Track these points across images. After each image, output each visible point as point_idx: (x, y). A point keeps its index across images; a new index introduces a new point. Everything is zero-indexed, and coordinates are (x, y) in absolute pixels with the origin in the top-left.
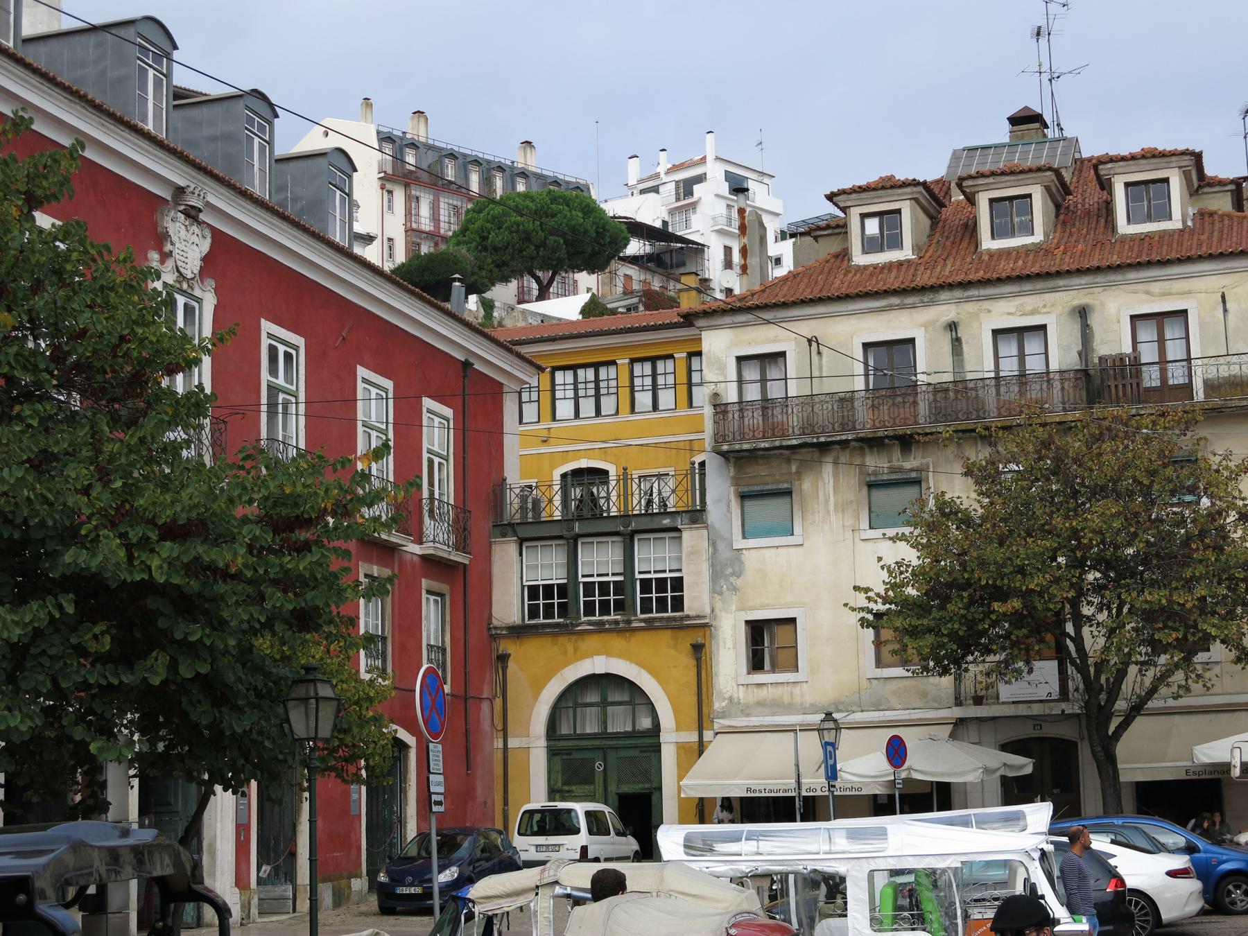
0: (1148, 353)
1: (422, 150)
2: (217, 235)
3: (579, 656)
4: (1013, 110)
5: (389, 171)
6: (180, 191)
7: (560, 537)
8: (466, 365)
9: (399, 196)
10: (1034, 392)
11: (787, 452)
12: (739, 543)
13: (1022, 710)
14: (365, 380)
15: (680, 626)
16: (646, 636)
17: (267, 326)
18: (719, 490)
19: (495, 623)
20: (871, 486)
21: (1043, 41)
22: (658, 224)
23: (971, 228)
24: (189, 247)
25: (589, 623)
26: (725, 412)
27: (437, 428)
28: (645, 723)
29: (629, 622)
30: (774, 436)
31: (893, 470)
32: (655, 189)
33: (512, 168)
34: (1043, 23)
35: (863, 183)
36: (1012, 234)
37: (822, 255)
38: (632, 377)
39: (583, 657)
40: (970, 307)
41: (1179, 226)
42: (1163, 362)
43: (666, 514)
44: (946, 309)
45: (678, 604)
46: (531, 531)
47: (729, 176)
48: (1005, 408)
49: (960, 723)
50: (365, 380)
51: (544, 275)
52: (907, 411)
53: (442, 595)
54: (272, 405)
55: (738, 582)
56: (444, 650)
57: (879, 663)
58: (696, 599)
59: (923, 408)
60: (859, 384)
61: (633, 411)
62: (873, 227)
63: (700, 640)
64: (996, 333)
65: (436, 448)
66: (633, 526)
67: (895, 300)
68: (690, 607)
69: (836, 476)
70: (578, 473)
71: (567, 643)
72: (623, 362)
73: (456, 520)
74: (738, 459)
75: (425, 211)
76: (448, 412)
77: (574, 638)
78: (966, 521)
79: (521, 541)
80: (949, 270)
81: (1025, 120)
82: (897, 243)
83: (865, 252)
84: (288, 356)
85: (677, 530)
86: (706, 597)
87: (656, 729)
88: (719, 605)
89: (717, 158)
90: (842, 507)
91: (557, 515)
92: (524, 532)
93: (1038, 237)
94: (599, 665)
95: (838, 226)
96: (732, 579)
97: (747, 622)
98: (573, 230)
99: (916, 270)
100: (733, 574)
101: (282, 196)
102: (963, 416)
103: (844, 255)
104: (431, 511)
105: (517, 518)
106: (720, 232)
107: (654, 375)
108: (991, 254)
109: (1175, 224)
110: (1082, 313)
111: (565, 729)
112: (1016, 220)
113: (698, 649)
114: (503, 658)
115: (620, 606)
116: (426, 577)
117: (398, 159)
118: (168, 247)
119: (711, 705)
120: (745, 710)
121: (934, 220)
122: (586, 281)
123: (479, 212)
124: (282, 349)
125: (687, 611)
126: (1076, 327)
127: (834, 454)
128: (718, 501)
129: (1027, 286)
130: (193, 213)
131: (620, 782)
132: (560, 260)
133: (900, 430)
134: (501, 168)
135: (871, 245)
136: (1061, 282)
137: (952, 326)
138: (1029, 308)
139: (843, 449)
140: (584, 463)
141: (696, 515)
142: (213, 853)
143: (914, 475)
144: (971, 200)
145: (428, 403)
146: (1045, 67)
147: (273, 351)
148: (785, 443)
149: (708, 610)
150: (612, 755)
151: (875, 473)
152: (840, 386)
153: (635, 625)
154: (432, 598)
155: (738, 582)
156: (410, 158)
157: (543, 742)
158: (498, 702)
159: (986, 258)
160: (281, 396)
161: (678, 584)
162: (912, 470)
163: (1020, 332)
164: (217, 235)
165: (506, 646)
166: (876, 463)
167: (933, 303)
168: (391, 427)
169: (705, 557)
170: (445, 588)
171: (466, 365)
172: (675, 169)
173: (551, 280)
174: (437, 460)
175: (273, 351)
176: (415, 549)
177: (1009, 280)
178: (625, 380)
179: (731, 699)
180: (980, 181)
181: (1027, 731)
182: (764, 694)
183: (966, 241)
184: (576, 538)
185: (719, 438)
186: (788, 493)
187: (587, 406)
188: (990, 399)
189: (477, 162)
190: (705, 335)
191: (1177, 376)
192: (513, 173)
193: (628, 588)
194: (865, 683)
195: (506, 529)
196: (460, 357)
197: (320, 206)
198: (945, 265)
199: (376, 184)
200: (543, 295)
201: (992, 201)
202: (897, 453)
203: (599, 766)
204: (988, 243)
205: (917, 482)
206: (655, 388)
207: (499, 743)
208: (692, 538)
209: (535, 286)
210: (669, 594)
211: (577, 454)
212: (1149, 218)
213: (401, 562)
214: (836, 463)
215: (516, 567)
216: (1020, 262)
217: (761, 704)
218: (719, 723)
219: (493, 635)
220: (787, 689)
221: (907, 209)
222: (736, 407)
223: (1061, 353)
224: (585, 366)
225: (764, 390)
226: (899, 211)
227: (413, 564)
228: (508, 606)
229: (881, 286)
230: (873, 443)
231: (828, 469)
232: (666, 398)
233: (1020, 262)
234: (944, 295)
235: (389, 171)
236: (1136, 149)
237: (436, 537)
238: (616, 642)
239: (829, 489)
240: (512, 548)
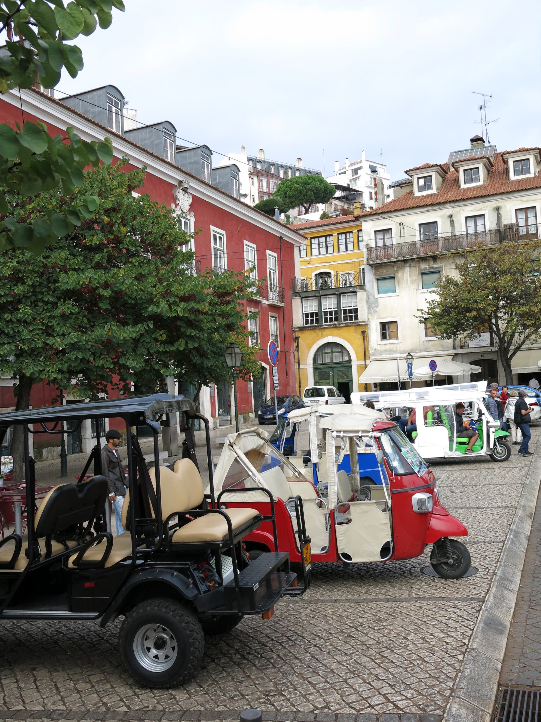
0: (522, 222)
1: (263, 163)
2: (194, 197)
3: (323, 337)
4: (472, 136)
5: (252, 171)
6: (181, 182)
7: (315, 296)
8: (281, 238)
9: (256, 179)
10: (480, 239)
11: (393, 264)
12: (377, 296)
13: (477, 350)
14: (246, 245)
15: (357, 325)
16: (346, 328)
17: (212, 228)
18: (370, 277)
19: (294, 326)
20: (422, 274)
21: (483, 110)
22: (346, 185)
23: (457, 181)
25: (326, 325)
26: (371, 250)
27: (272, 260)
28: (346, 358)
29: (340, 324)
30: (388, 258)
31: (430, 268)
32: (345, 173)
33: (294, 168)
34: (483, 104)
35: (418, 166)
36: (472, 182)
37: (404, 193)
38: (338, 240)
39: (324, 337)
40: (457, 209)
41: (533, 176)
42: (527, 225)
43: (351, 286)
44: (448, 210)
45: (356, 317)
46: (305, 294)
47: (371, 167)
48: (470, 245)
49: (455, 355)
50: (246, 245)
51: (307, 205)
52: (435, 247)
53: (276, 318)
54: (216, 255)
55: (377, 309)
56: (277, 336)
57: (427, 335)
58: (362, 316)
59: (441, 246)
60: (418, 238)
61: (339, 251)
62: (422, 182)
63: (364, 330)
64: (466, 218)
65: (272, 267)
66: (340, 291)
67: (430, 208)
68: (360, 318)
69: (410, 271)
70: (320, 274)
71: (318, 332)
72: (335, 234)
73: (280, 292)
74: (376, 267)
75: (265, 184)
77: (321, 330)
78: (456, 285)
79: (302, 298)
80: (449, 196)
81: (477, 140)
82: (430, 187)
83: (419, 191)
84: (220, 238)
85: (355, 292)
86: (366, 315)
87: (350, 360)
88: (370, 318)
90: (412, 282)
91: (314, 289)
92: (303, 295)
93: (481, 182)
95: (409, 183)
96: (375, 308)
97: (380, 323)
98: (316, 189)
100: (375, 307)
101: (215, 182)
102: (455, 249)
103: (411, 193)
104: (271, 289)
105: (300, 290)
106: (368, 187)
107: (346, 239)
108: (464, 190)
109: (532, 175)
110: (498, 209)
111: (319, 362)
112: (473, 177)
113: (363, 333)
114: (297, 338)
115: (336, 319)
116: (270, 312)
117: (255, 167)
118: (177, 202)
119: (369, 351)
120: (380, 353)
121: (444, 178)
122: (322, 207)
123: (284, 184)
124: (218, 235)
125: (359, 320)
126: (495, 214)
127: (409, 263)
128: (369, 281)
129: (477, 201)
130: (185, 189)
131: (338, 379)
132: (312, 200)
133: (432, 254)
134: (290, 168)
135: (421, 189)
136: (490, 198)
137: (451, 216)
138: (478, 208)
139: (413, 261)
140: (322, 270)
141: (362, 287)
142: (203, 406)
143: (438, 269)
144: (457, 170)
145: (268, 252)
146: (484, 120)
147: (215, 236)
148: (392, 260)
149: (366, 320)
150: (335, 370)
151: (424, 270)
152: (411, 240)
153: (342, 325)
154: (272, 318)
155: (377, 309)
156: (259, 166)
157: (312, 366)
158: (296, 353)
159: (462, 191)
160: (218, 252)
161: (356, 311)
162: (437, 268)
163: (475, 217)
164: (194, 197)
165: (298, 334)
166: (424, 266)
167: (443, 208)
168: (256, 260)
169: (365, 301)
170: (276, 315)
171: (281, 238)
172: (352, 165)
173: (309, 207)
174: (272, 271)
175: (215, 236)
176: (266, 302)
177: (471, 198)
178: (336, 241)
179: (375, 349)
180: (460, 163)
181: (479, 357)
182: (386, 347)
183: (455, 185)
184: (321, 296)
185: (369, 259)
186: (394, 278)
187: (323, 251)
188: (464, 241)
189: (282, 166)
190: (363, 224)
191: (532, 230)
192: (295, 170)
193: (339, 313)
194: (422, 343)
195: (297, 294)
197: (229, 184)
198: (448, 195)
199: (248, 176)
200: (307, 212)
201: (464, 170)
202: (431, 262)
203: (331, 374)
204: (463, 186)
205: (439, 272)
207: (297, 367)
208: (361, 295)
209: (304, 209)
210: (328, 317)
211: (320, 267)
212: (522, 174)
213: (262, 307)
214: (410, 266)
215: (301, 307)
217: (386, 351)
218: (372, 358)
219: (294, 330)
220: (395, 345)
221: (434, 175)
222: (375, 249)
223: (490, 224)
224: (322, 236)
225: (384, 242)
226: (431, 176)
227: (266, 308)
228: (298, 321)
229: (425, 203)
230: (423, 259)
231: (407, 269)
232: (350, 247)
234: (448, 205)
235: (252, 171)
236: (517, 148)
237: (273, 298)
238: (335, 331)
239: (408, 277)
240: (299, 300)
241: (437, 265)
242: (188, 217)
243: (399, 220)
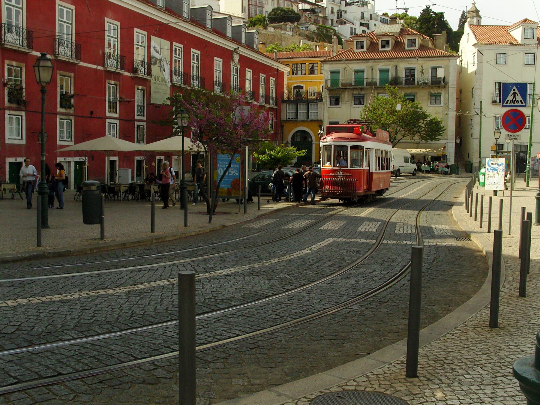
3: (297, 126)
6: (235, 49)
8: (278, 69)
24: (236, 58)
28: (310, 140)
44: (371, 63)
46: (289, 101)
72: (307, 63)
76: (274, 79)
94: (301, 128)
114: (283, 126)
140: (298, 85)
145: (271, 78)
164: (241, 55)
166: (356, 92)
171: (278, 69)
177: (383, 59)
202: (360, 91)
204: (380, 49)
231: (347, 93)
234: (370, 61)
241: (362, 93)
243: (344, 66)
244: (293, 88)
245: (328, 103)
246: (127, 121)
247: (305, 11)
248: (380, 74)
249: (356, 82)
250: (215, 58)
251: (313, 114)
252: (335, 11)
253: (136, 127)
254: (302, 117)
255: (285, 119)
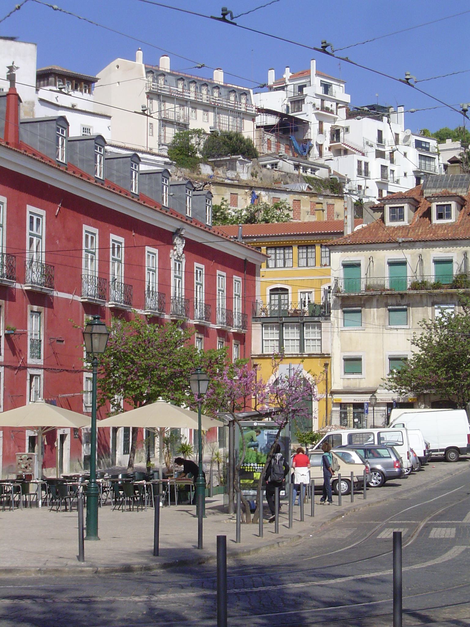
8: (246, 260)
24: (179, 245)
32: (283, 88)
63: (327, 362)
66: (304, 320)
70: (276, 289)
89: (318, 74)
93: (452, 220)
99: (409, 231)
113: (326, 365)
133: (401, 292)
140: (279, 286)
165: (256, 362)
171: (246, 260)
196: (243, 258)
198: (419, 229)
204: (435, 221)
206: (307, 258)
214: (378, 300)
216: (446, 231)
221: (406, 206)
233: (446, 231)
242: (181, 260)
243: (368, 253)
244: (268, 292)
245: (341, 322)
246: (15, 368)
247: (268, 128)
248: (436, 268)
249: (391, 283)
250: (147, 248)
251: (312, 343)
252: (327, 127)
253: (28, 377)
254: (291, 348)
255: (260, 353)
